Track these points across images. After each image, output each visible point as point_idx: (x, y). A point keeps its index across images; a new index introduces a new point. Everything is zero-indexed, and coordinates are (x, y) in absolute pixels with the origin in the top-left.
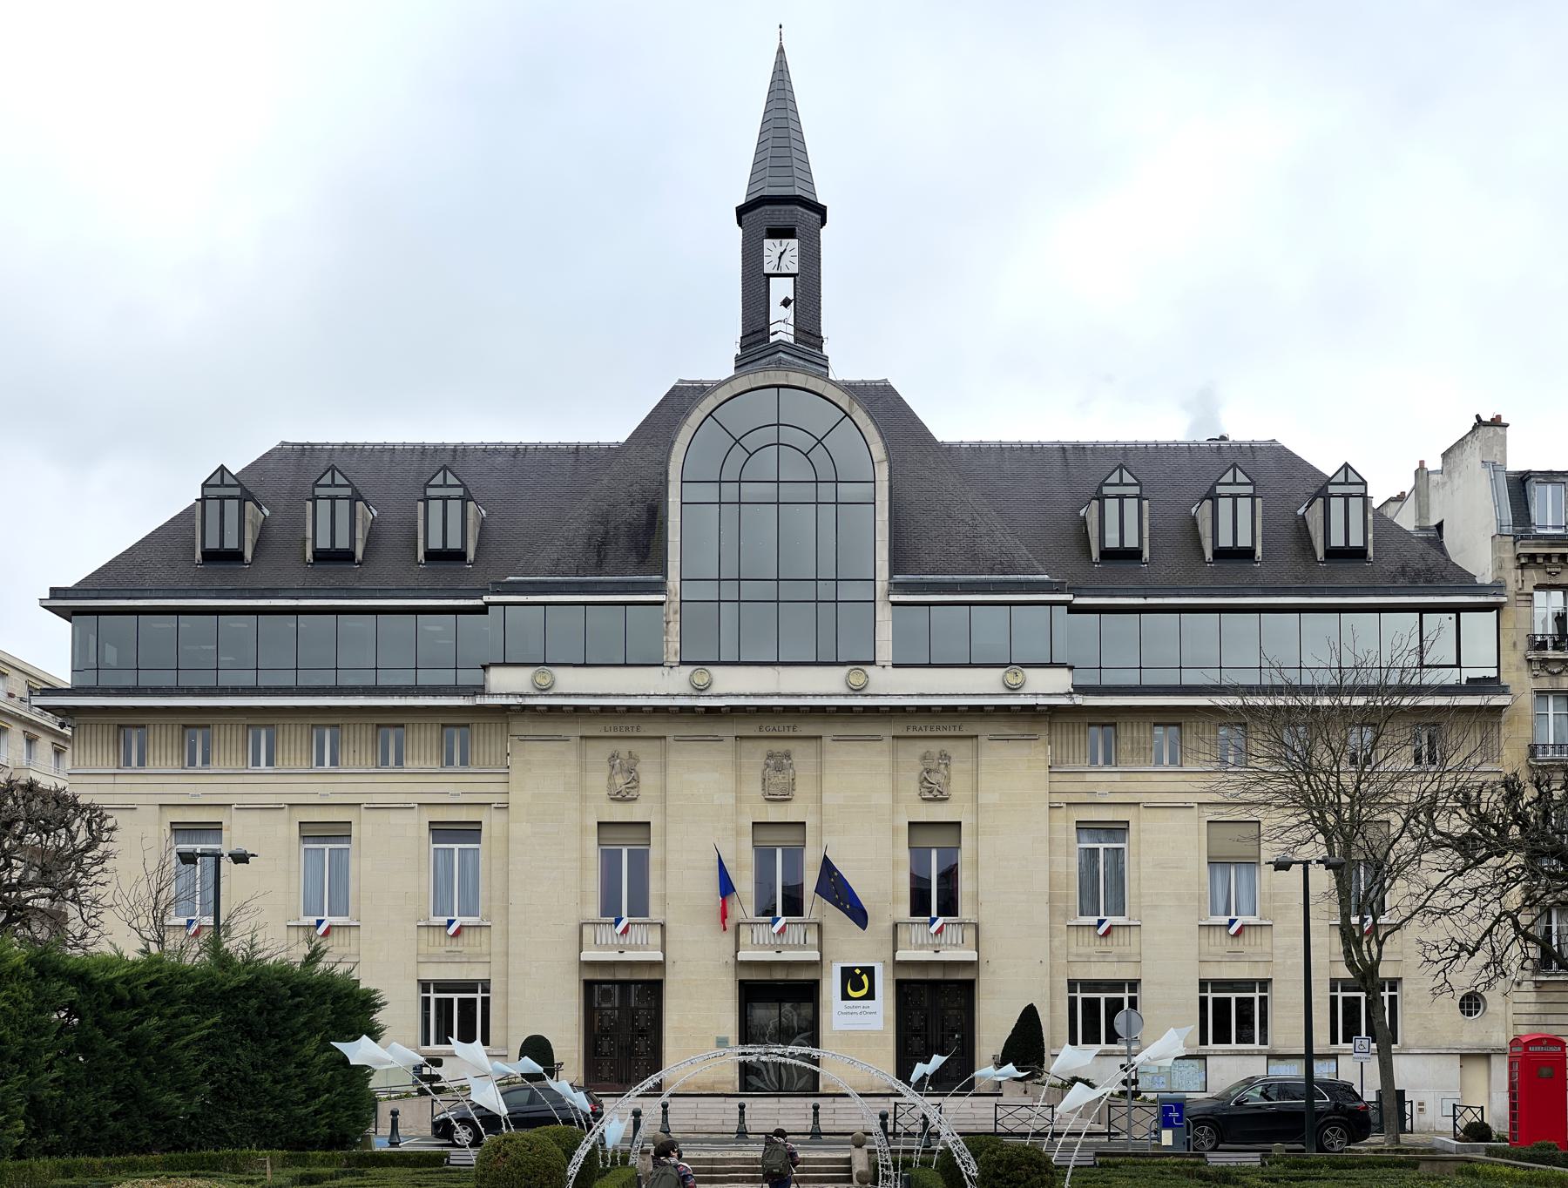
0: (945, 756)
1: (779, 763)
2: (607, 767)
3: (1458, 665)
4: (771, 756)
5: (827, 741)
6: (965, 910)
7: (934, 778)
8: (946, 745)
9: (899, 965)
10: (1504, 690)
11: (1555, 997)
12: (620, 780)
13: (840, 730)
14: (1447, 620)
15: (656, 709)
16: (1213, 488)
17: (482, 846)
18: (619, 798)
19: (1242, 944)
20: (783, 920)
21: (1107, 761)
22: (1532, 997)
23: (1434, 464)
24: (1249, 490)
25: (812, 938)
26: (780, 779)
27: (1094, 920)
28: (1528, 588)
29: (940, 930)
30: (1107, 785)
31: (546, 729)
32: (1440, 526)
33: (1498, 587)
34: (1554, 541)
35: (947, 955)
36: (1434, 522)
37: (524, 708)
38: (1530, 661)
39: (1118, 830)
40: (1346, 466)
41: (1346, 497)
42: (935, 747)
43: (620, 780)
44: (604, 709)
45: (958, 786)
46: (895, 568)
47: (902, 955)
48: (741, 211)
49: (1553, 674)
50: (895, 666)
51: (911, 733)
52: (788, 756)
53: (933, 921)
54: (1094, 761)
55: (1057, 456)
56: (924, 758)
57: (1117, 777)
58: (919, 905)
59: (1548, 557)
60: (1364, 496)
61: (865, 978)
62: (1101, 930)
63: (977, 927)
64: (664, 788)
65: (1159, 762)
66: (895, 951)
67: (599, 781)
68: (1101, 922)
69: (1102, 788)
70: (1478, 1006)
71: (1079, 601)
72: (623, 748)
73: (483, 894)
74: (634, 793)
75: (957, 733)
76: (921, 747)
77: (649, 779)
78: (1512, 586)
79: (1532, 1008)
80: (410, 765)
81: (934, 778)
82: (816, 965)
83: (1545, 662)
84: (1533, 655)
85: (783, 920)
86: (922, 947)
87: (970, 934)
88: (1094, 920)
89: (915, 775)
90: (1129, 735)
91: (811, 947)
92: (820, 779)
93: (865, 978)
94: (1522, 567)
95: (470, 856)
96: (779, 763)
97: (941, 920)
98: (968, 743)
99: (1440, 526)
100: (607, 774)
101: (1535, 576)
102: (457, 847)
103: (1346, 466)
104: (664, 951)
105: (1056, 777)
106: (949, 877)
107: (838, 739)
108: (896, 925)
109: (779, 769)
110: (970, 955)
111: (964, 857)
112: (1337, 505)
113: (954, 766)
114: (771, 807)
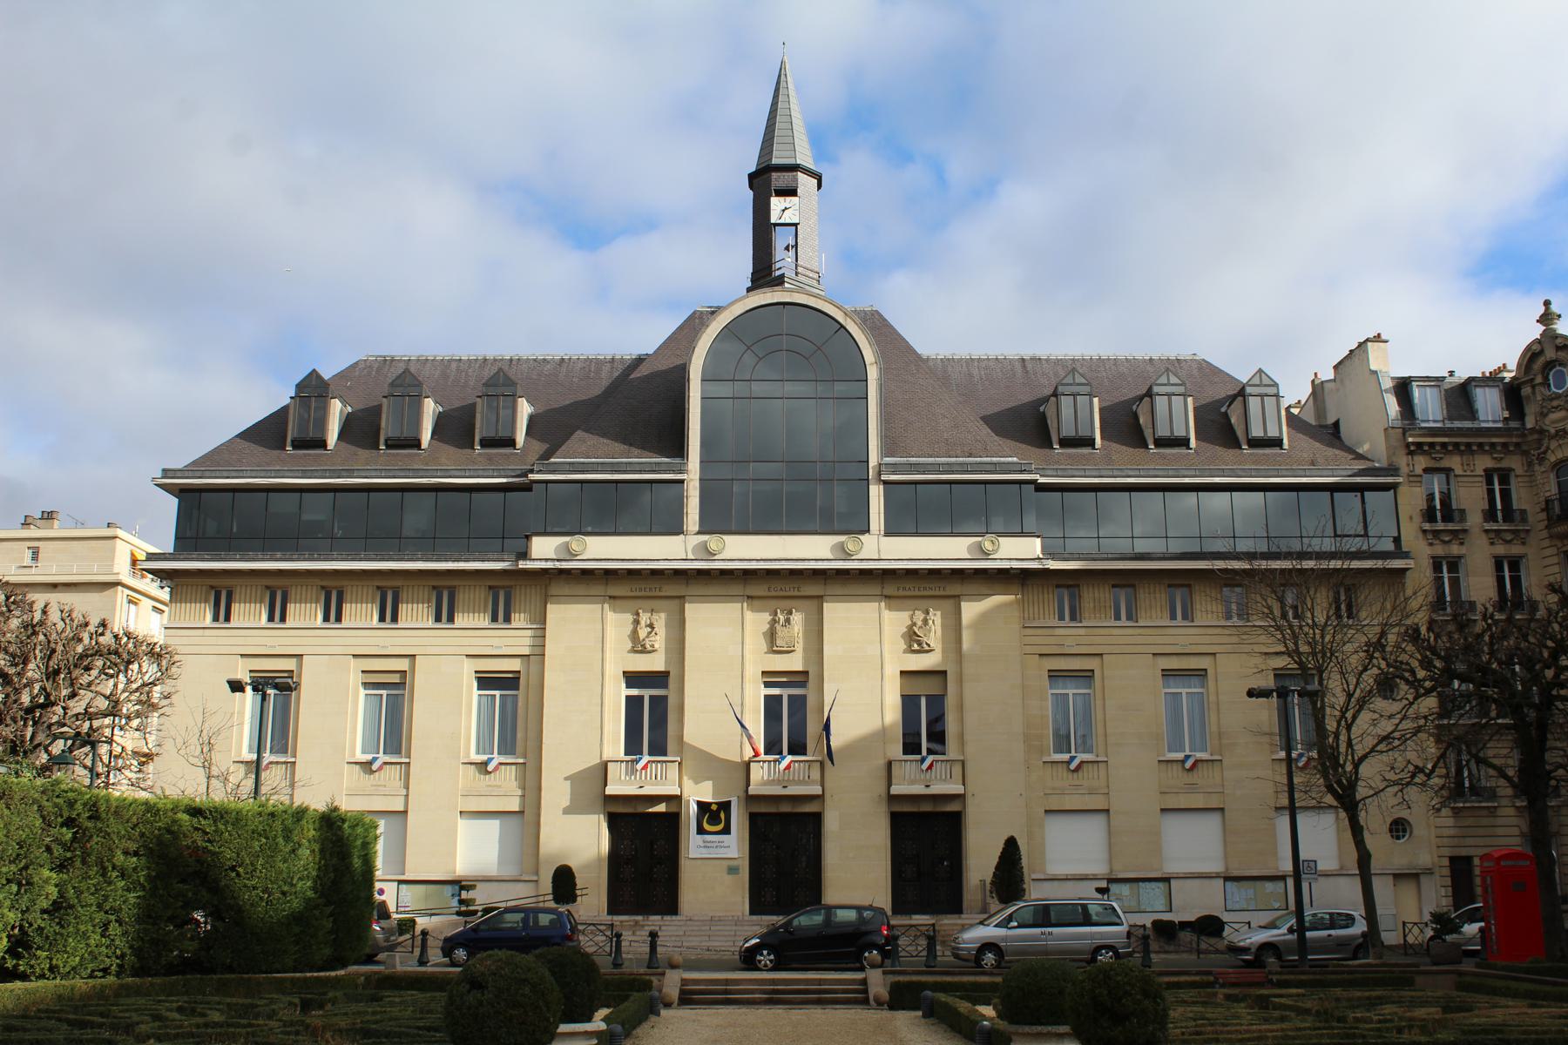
3: (1366, 535)
6: (952, 750)
9: (892, 799)
10: (1406, 555)
11: (1470, 821)
13: (838, 590)
14: (1353, 499)
15: (677, 572)
16: (1150, 388)
17: (521, 693)
19: (1194, 778)
21: (1073, 618)
22: (1450, 822)
23: (1327, 374)
24: (1181, 389)
25: (816, 774)
27: (1066, 757)
28: (1418, 470)
29: (930, 767)
30: (1072, 636)
31: (580, 589)
32: (1336, 424)
33: (1392, 470)
34: (1433, 432)
35: (937, 789)
36: (1331, 420)
37: (561, 571)
38: (1424, 532)
39: (1086, 676)
40: (1260, 371)
41: (1262, 396)
44: (630, 572)
46: (888, 447)
47: (895, 790)
48: (752, 177)
49: (1444, 542)
50: (887, 534)
51: (901, 593)
53: (923, 760)
54: (1061, 618)
55: (1018, 366)
57: (1082, 632)
58: (911, 747)
59: (1432, 445)
60: (1277, 396)
62: (1073, 766)
63: (963, 763)
65: (1118, 618)
66: (889, 784)
68: (1073, 758)
69: (1069, 641)
70: (1404, 831)
71: (1042, 480)
73: (520, 735)
75: (942, 593)
78: (1404, 470)
79: (1452, 832)
80: (461, 620)
83: (1436, 533)
84: (1427, 526)
85: (789, 758)
86: (913, 782)
87: (957, 769)
88: (1066, 757)
90: (1091, 596)
94: (1411, 453)
95: (509, 701)
97: (931, 758)
99: (1336, 424)
101: (1421, 462)
102: (497, 693)
103: (1260, 371)
105: (1029, 632)
106: (937, 720)
108: (890, 764)
110: (955, 788)
111: (950, 701)
112: (1254, 403)
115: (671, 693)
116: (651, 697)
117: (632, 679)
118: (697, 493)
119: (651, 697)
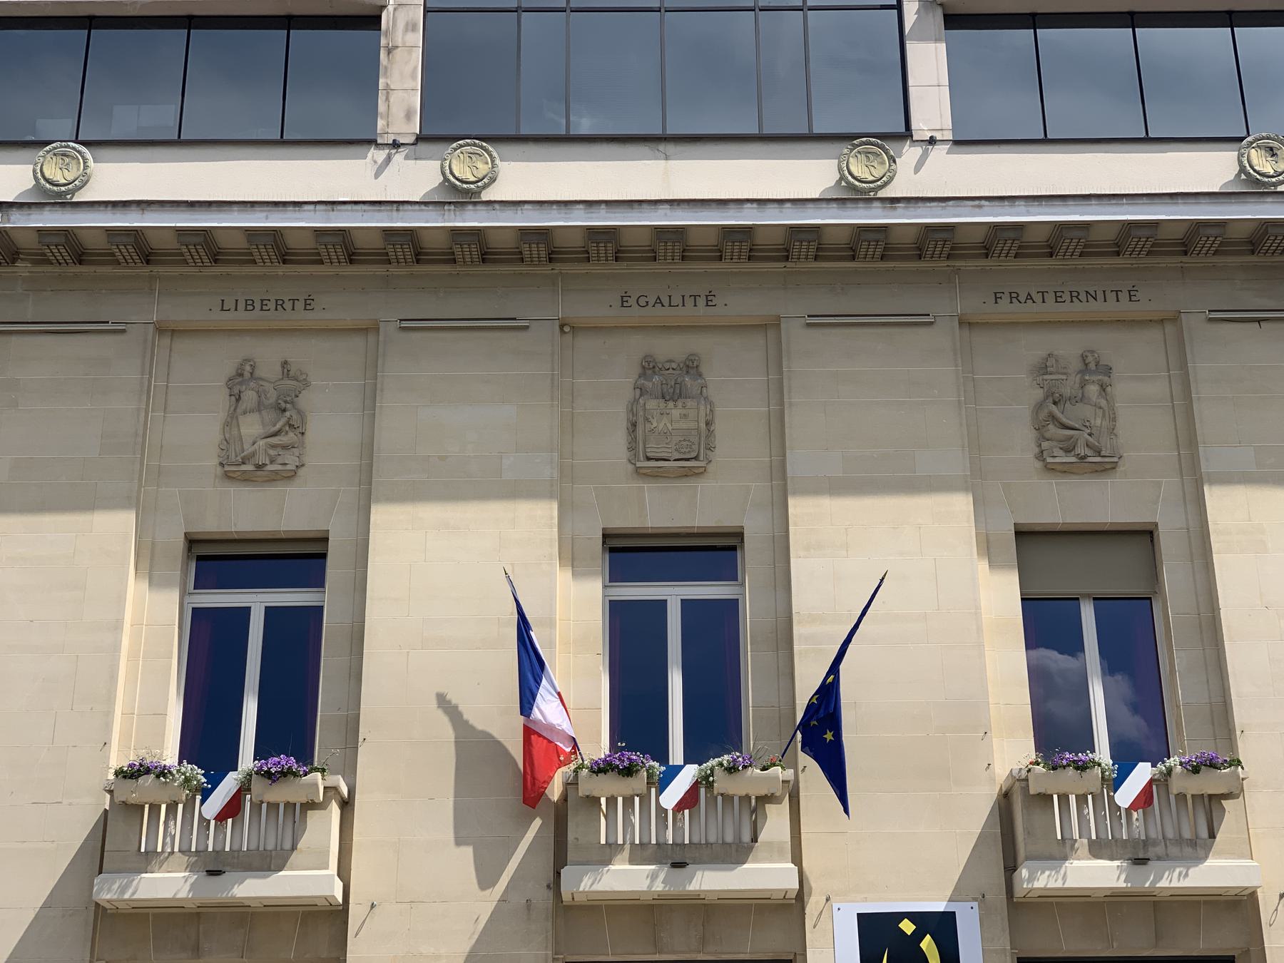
0: (1095, 369)
1: (671, 382)
2: (222, 400)
4: (649, 367)
5: (794, 333)
7: (1071, 414)
8: (1104, 343)
12: (251, 427)
18: (241, 469)
20: (689, 774)
26: (671, 421)
42: (1068, 345)
43: (251, 427)
45: (1140, 423)
52: (691, 366)
56: (1043, 369)
61: (927, 944)
64: (368, 450)
67: (196, 431)
72: (269, 355)
74: (291, 459)
76: (1033, 346)
77: (329, 427)
81: (1071, 414)
82: (791, 909)
89: (1024, 410)
91: (773, 853)
92: (778, 393)
93: (927, 944)
96: (671, 382)
98: (1154, 334)
100: (222, 415)
104: (344, 872)
107: (817, 322)
109: (674, 394)
113: (1122, 389)
114: (649, 489)
115: (330, 600)
116: (270, 612)
117: (214, 560)
118: (417, 38)
119: (270, 612)
